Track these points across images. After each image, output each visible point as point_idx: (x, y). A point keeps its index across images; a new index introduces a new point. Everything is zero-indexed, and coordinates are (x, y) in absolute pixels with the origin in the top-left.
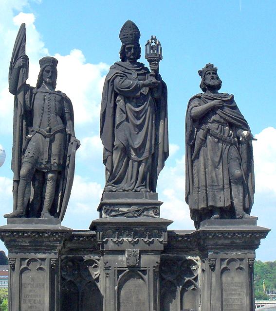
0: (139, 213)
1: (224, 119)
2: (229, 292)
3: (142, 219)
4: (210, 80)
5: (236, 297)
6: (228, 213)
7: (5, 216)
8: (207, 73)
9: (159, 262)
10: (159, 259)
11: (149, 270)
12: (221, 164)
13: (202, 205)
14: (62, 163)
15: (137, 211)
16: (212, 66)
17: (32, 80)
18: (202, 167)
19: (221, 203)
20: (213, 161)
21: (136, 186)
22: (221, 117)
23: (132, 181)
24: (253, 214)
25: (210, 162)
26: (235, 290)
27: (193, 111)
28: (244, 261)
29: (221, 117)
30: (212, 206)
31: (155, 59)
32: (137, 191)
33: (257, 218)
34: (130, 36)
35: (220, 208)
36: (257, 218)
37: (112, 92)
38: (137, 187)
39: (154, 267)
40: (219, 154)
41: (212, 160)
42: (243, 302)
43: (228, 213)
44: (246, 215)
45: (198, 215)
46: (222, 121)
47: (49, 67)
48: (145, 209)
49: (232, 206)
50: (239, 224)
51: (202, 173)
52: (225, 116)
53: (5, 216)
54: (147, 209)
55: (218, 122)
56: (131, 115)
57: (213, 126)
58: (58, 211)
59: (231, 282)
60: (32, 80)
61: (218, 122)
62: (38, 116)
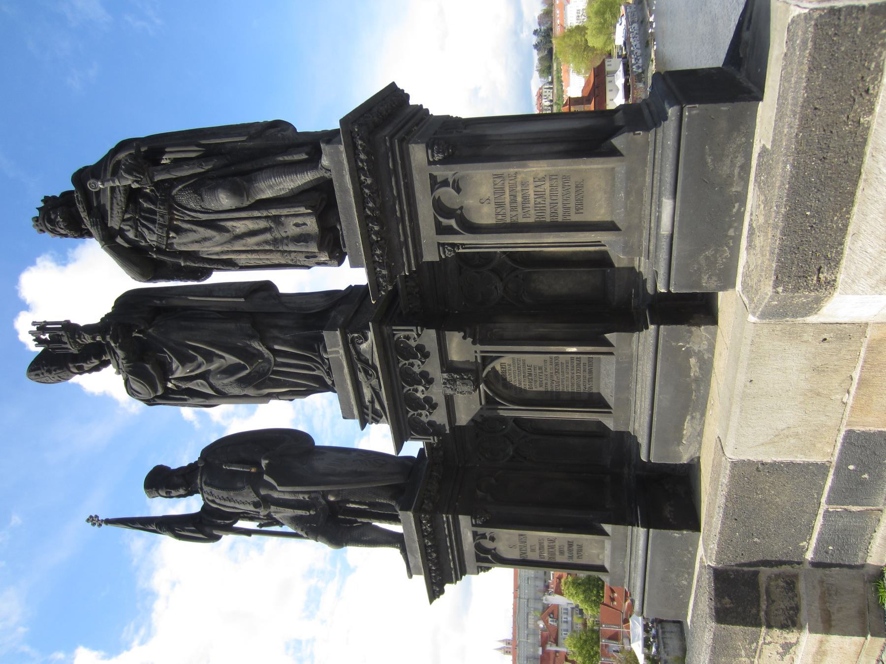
0: (368, 367)
2: (520, 209)
5: (531, 192)
9: (462, 334)
10: (456, 333)
11: (482, 352)
15: (366, 373)
19: (309, 223)
26: (513, 197)
28: (435, 173)
35: (320, 221)
39: (474, 343)
42: (541, 175)
48: (360, 360)
54: (358, 353)
59: (493, 205)
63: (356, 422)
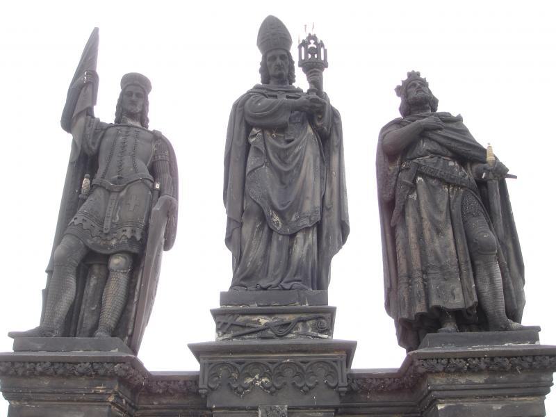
1: (449, 149)
3: (292, 338)
4: (416, 97)
6: (476, 318)
7: (11, 335)
8: (410, 84)
12: (450, 226)
13: (420, 308)
14: (138, 237)
16: (418, 74)
17: (105, 110)
18: (412, 235)
20: (432, 219)
21: (285, 280)
22: (441, 144)
23: (278, 271)
24: (527, 320)
25: (427, 224)
27: (386, 138)
29: (441, 144)
30: (438, 308)
31: (315, 67)
32: (284, 289)
33: (538, 329)
34: (273, 38)
36: (538, 329)
37: (240, 123)
38: (287, 282)
40: (443, 207)
41: (431, 221)
43: (476, 318)
44: (515, 324)
45: (413, 330)
46: (445, 151)
47: (135, 92)
49: (480, 307)
50: (501, 340)
51: (413, 246)
52: (449, 142)
53: (11, 335)
55: (435, 153)
56: (274, 156)
57: (428, 161)
58: (130, 332)
60: (105, 110)
61: (435, 153)
62: (104, 160)
63: (217, 306)
